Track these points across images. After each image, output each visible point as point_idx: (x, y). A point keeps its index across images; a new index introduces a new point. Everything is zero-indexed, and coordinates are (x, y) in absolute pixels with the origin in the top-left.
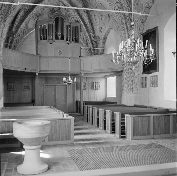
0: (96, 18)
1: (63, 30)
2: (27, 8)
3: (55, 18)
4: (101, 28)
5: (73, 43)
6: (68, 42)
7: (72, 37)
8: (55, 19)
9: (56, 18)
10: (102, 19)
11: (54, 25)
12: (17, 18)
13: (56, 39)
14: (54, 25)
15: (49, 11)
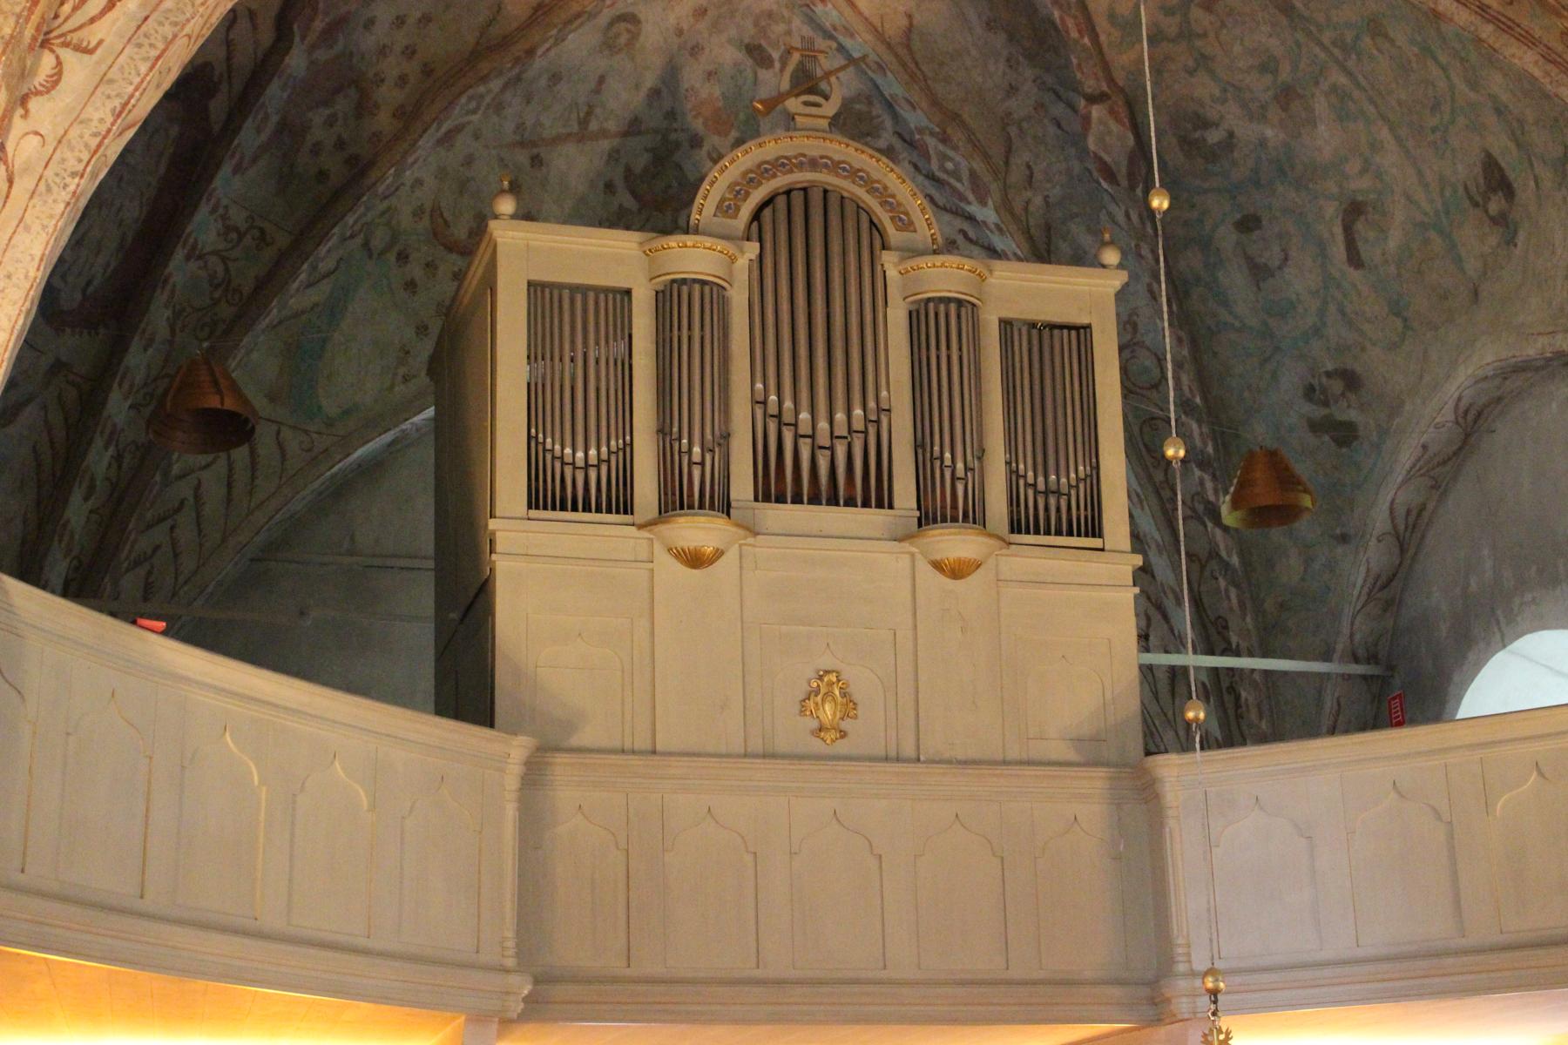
0: (1272, 256)
1: (863, 379)
2: (330, 122)
3: (758, 196)
4: (1337, 386)
5: (1035, 559)
6: (955, 543)
7: (1013, 475)
8: (756, 216)
9: (768, 202)
10: (1355, 259)
11: (739, 298)
12: (179, 254)
13: (770, 490)
14: (739, 298)
15: (609, 187)
